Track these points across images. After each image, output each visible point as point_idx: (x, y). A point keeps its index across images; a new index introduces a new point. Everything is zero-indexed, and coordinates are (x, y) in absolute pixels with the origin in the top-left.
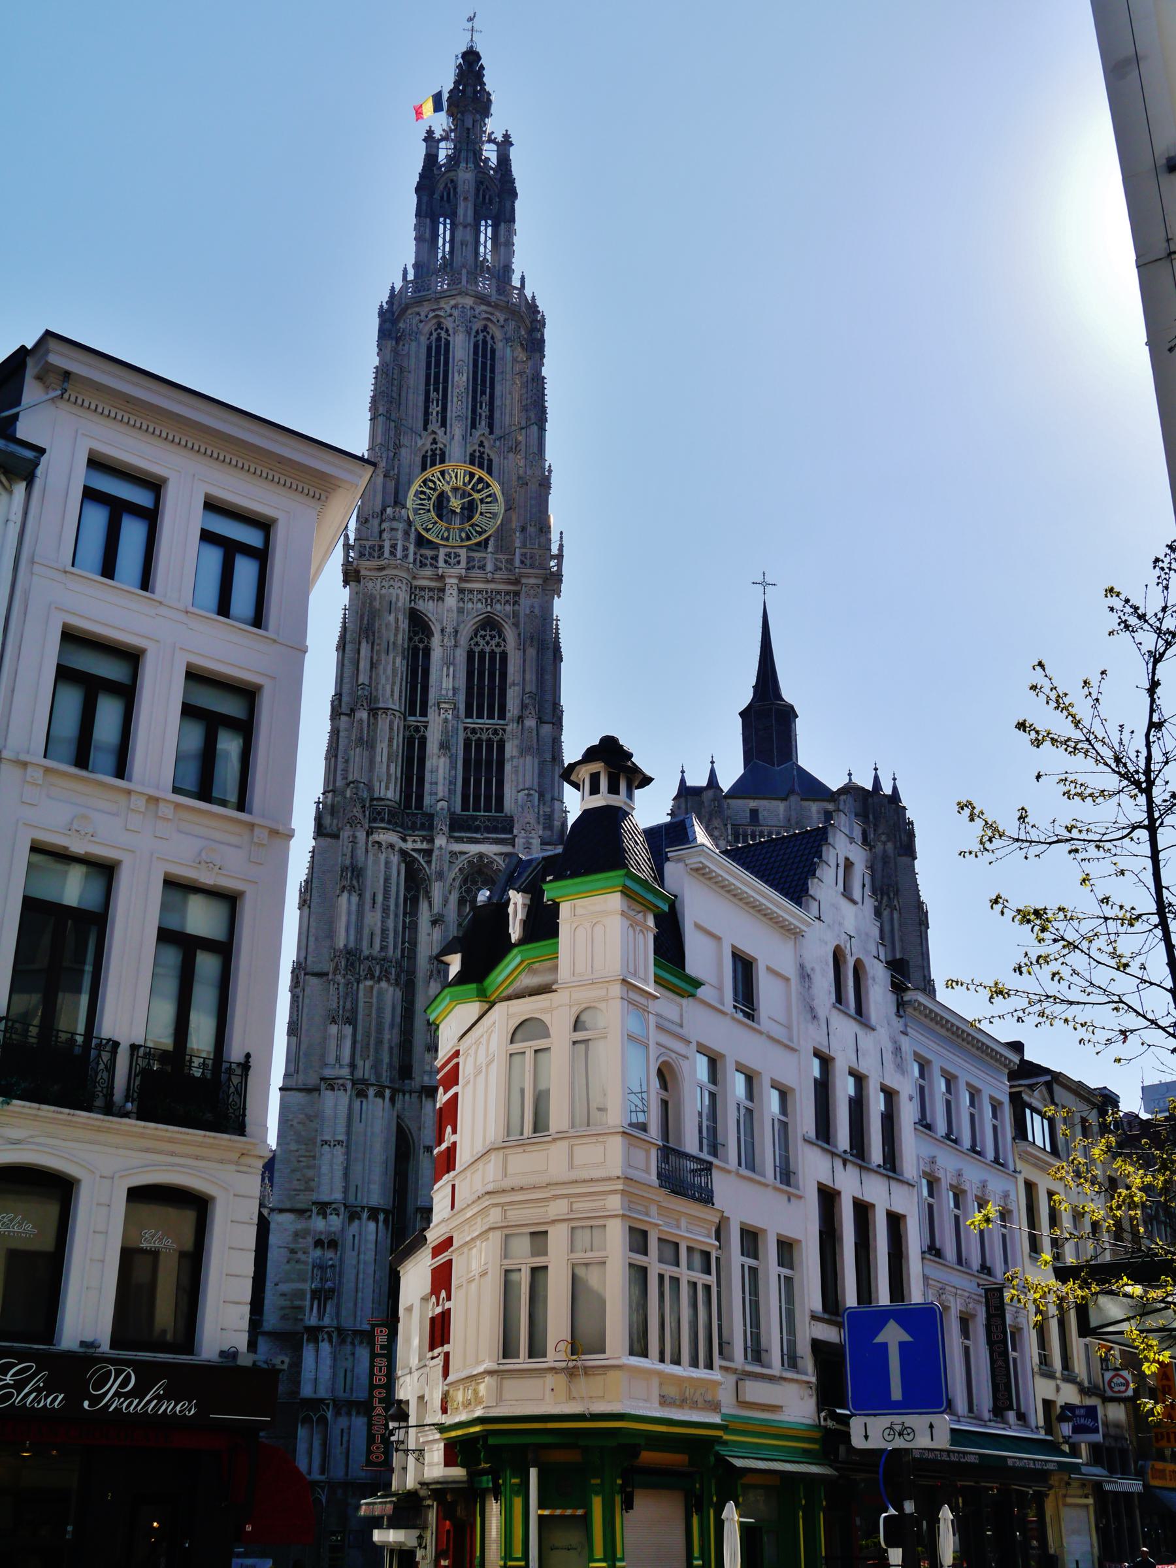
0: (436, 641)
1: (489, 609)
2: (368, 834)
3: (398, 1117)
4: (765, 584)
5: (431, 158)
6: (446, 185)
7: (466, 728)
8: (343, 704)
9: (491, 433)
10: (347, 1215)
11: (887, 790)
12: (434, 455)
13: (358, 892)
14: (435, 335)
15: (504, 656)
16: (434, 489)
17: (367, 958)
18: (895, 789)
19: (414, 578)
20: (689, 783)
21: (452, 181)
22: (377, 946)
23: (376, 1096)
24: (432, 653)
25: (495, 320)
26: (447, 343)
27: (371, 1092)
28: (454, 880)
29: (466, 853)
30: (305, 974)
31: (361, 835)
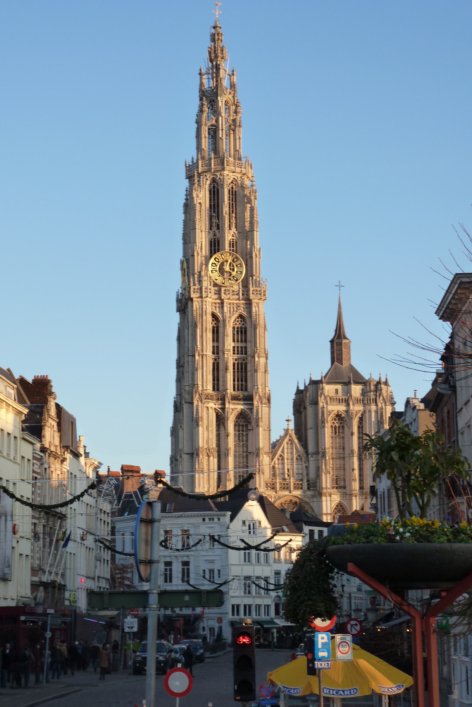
0: (221, 325)
4: (340, 286)
5: (201, 84)
6: (210, 102)
8: (190, 352)
11: (383, 380)
12: (215, 241)
14: (212, 186)
15: (246, 328)
16: (218, 262)
17: (206, 449)
18: (386, 379)
20: (314, 378)
21: (213, 101)
24: (219, 329)
25: (236, 178)
26: (218, 190)
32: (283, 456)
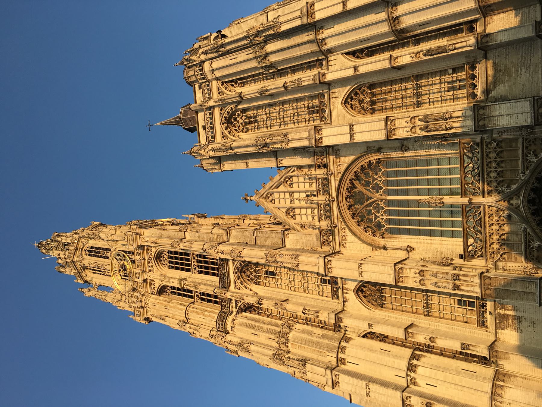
1: (152, 259)
2: (228, 333)
3: (359, 336)
7: (195, 273)
9: (110, 250)
10: (413, 387)
13: (249, 345)
14: (90, 270)
19: (147, 292)
22: (272, 336)
23: (344, 353)
27: (341, 355)
28: (246, 288)
29: (235, 281)
30: (295, 374)
31: (228, 337)
32: (289, 209)
